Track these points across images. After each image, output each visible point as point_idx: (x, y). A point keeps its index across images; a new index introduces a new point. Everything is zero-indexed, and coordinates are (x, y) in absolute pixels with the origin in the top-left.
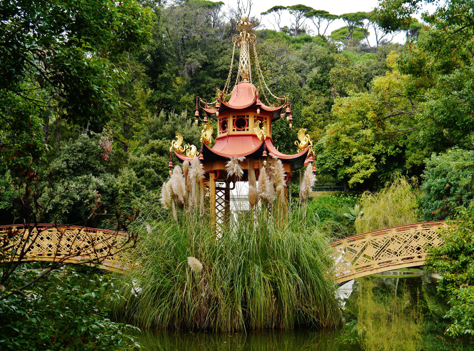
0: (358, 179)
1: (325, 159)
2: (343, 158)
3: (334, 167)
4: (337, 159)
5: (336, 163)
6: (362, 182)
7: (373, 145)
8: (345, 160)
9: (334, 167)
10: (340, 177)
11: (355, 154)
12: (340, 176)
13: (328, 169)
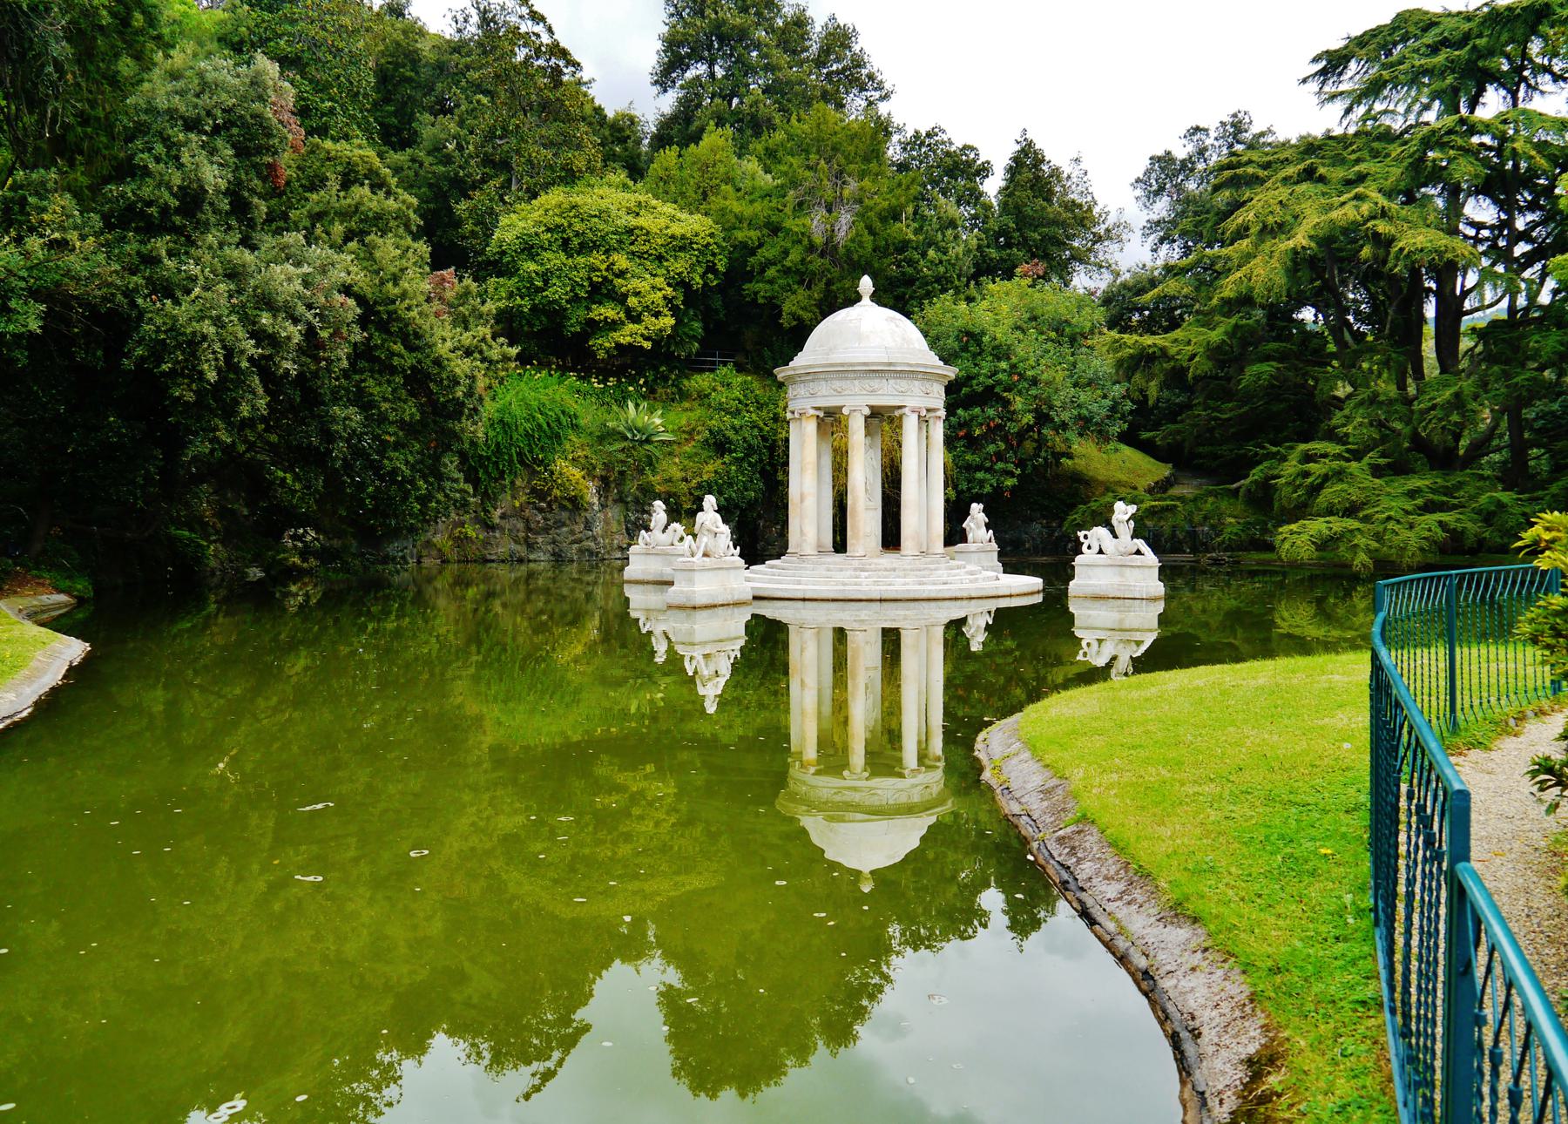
0: (639, 339)
1: (546, 277)
2: (590, 279)
3: (567, 301)
6: (647, 345)
7: (660, 258)
8: (592, 284)
9: (567, 301)
10: (573, 326)
11: (621, 274)
12: (572, 326)
13: (555, 301)
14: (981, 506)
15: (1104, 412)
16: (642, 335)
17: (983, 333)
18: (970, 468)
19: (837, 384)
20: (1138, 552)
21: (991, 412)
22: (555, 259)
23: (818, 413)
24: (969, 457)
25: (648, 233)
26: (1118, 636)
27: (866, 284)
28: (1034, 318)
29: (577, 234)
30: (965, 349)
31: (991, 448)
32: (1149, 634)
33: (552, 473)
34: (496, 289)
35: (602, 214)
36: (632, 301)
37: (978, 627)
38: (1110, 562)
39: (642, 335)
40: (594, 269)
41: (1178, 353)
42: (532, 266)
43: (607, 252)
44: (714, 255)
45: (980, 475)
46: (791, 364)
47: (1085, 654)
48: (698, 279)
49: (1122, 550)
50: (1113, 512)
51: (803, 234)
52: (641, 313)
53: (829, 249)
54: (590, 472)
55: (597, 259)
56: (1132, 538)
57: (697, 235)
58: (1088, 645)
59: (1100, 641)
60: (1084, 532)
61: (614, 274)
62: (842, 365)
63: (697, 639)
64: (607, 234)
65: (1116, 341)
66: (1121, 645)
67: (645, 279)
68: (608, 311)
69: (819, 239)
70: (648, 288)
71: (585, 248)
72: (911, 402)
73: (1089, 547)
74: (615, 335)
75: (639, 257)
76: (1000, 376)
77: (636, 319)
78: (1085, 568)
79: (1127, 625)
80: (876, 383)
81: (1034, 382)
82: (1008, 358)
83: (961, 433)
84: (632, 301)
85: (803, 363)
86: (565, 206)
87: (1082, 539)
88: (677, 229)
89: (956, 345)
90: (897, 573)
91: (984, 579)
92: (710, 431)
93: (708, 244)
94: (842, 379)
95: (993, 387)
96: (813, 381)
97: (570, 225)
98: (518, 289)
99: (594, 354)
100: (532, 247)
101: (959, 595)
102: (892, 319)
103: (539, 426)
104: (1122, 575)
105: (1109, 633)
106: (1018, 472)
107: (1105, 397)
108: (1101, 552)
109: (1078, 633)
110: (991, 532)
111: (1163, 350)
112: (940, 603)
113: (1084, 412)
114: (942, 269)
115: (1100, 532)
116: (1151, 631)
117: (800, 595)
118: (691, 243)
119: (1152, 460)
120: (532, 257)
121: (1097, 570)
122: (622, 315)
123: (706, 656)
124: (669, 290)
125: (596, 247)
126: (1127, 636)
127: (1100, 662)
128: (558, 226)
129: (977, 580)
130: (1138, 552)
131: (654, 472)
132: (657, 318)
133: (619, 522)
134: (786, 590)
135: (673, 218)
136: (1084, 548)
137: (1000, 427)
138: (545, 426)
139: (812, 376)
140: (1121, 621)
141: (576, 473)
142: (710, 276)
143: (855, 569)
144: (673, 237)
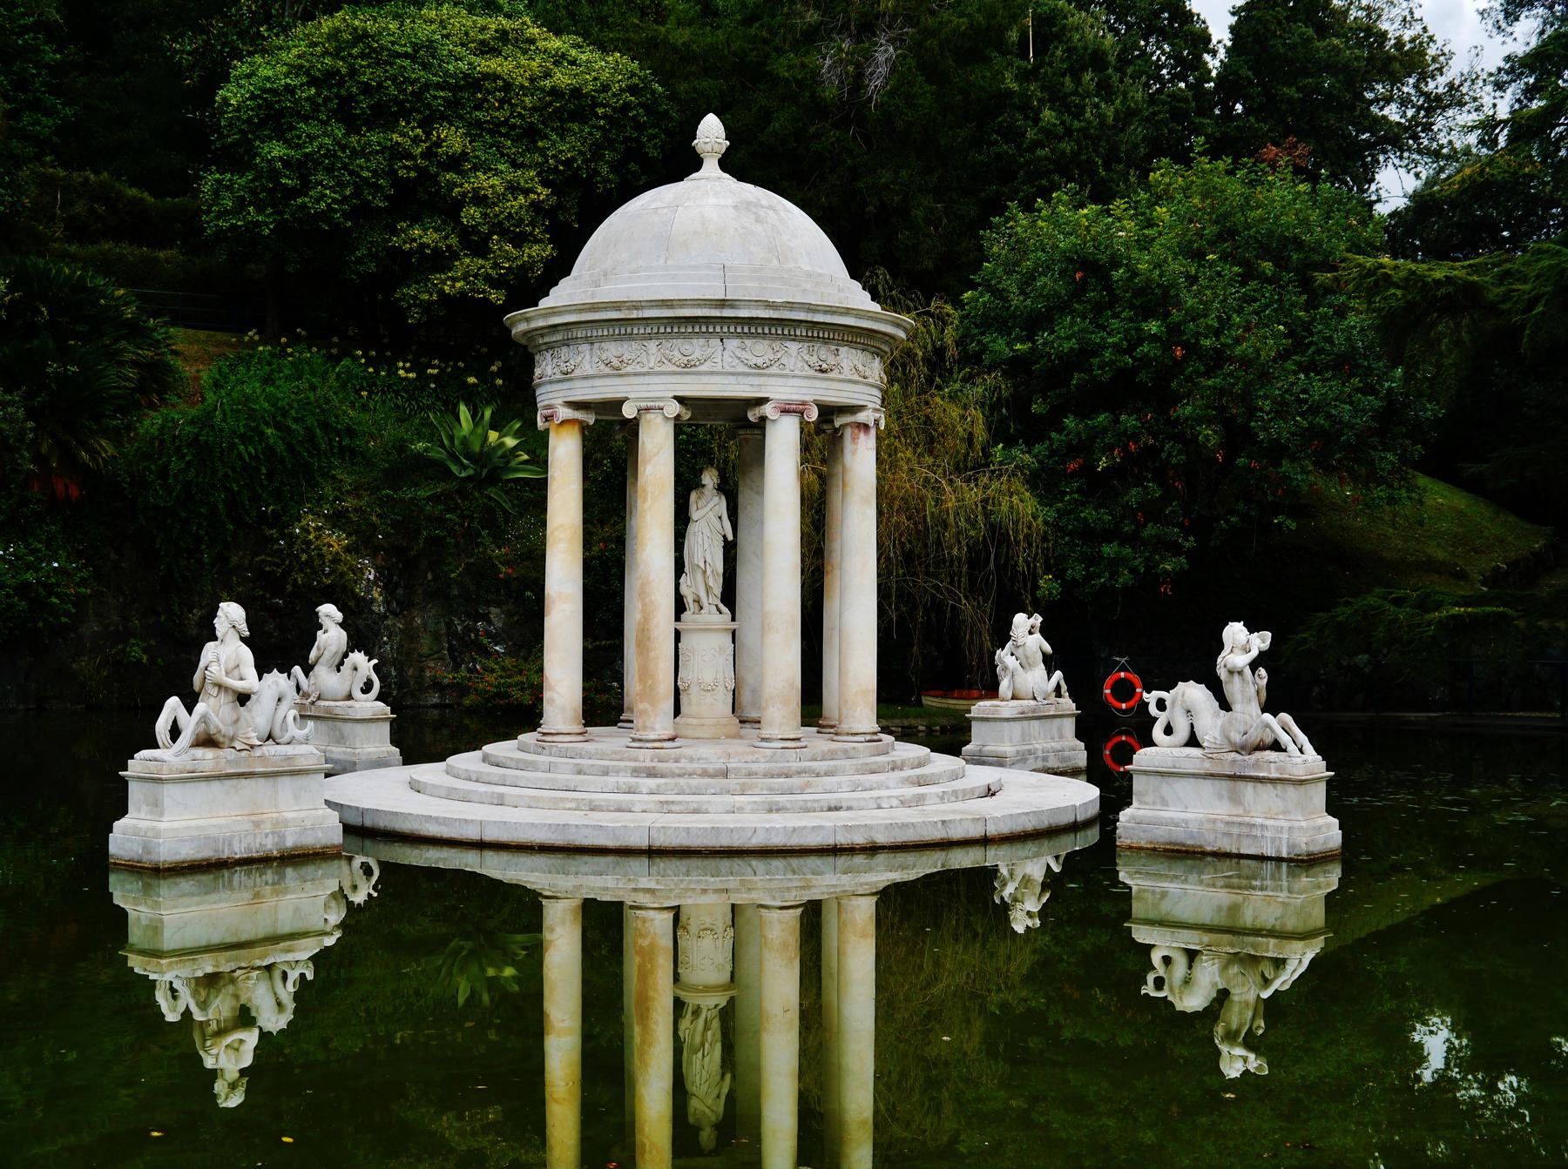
0: (481, 285)
1: (303, 168)
2: (392, 173)
3: (345, 215)
4: (365, 174)
5: (357, 193)
7: (530, 134)
8: (397, 182)
9: (345, 215)
11: (455, 163)
12: (359, 261)
13: (321, 215)
14: (1037, 619)
15: (1362, 421)
16: (488, 279)
17: (1115, 263)
18: (1092, 535)
19: (612, 350)
20: (1276, 746)
21: (1128, 421)
22: (321, 137)
23: (579, 415)
24: (1087, 513)
25: (508, 87)
26: (1227, 945)
27: (711, 132)
28: (1227, 234)
29: (367, 89)
30: (1078, 292)
31: (1134, 496)
32: (1298, 945)
33: (291, 538)
34: (216, 193)
35: (424, 52)
36: (471, 214)
37: (1026, 881)
38: (1208, 767)
39: (488, 279)
40: (397, 153)
41: (1506, 297)
42: (277, 150)
43: (427, 124)
44: (639, 127)
45: (1108, 550)
46: (544, 303)
47: (1159, 984)
48: (605, 170)
49: (1237, 738)
50: (1220, 646)
51: (800, 83)
52: (491, 233)
53: (852, 107)
54: (363, 542)
55: (405, 134)
56: (1263, 711)
57: (605, 88)
58: (1167, 960)
59: (1192, 955)
60: (1156, 694)
61: (440, 164)
62: (617, 306)
63: (169, 941)
64: (427, 86)
65: (1371, 272)
66: (1234, 970)
67: (497, 173)
68: (424, 235)
69: (830, 90)
70: (500, 190)
71: (385, 115)
72: (779, 390)
73: (1168, 730)
74: (437, 278)
75: (492, 133)
76: (1145, 348)
77: (481, 250)
78: (1152, 780)
79: (1247, 918)
80: (696, 348)
81: (1218, 359)
82: (1167, 314)
83: (1072, 466)
84: (471, 214)
85: (554, 311)
86: (347, 36)
87: (1153, 710)
88: (562, 78)
89: (1061, 288)
90: (732, 782)
91: (942, 797)
92: (614, 462)
93: (627, 107)
94: (621, 338)
95: (1135, 371)
96: (566, 343)
97: (353, 72)
98: (253, 192)
99: (403, 314)
100: (281, 113)
101: (843, 839)
102: (749, 206)
103: (270, 450)
104: (1235, 800)
105: (1206, 938)
106: (1190, 543)
107: (1369, 390)
108: (1193, 741)
109: (1141, 935)
110: (1058, 675)
111: (1470, 289)
112: (795, 862)
113: (1320, 420)
114: (1067, 146)
115: (1192, 693)
116: (1305, 936)
117: (472, 834)
118: (595, 104)
119: (1512, 519)
120: (280, 134)
121: (1183, 787)
122: (454, 240)
123: (211, 982)
124: (544, 192)
125: (406, 114)
126: (1248, 946)
127: (1192, 1002)
128: (330, 74)
129: (920, 800)
130: (1276, 746)
131: (498, 539)
132: (518, 246)
133: (436, 637)
134: (445, 821)
135: (560, 58)
136: (1157, 732)
137: (1153, 452)
138: (281, 448)
139: (568, 334)
140: (1234, 909)
141: (336, 541)
142: (633, 167)
143: (636, 772)
144: (555, 92)
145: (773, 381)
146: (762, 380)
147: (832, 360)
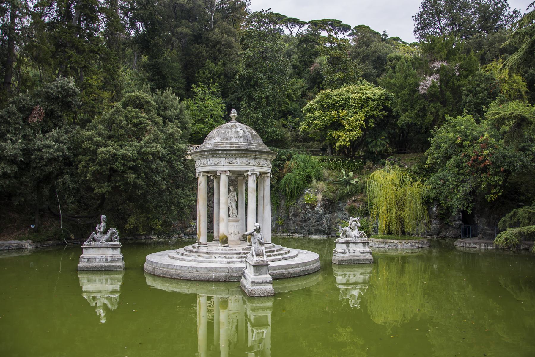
145: (218, 167)
146: (216, 167)
147: (234, 161)
